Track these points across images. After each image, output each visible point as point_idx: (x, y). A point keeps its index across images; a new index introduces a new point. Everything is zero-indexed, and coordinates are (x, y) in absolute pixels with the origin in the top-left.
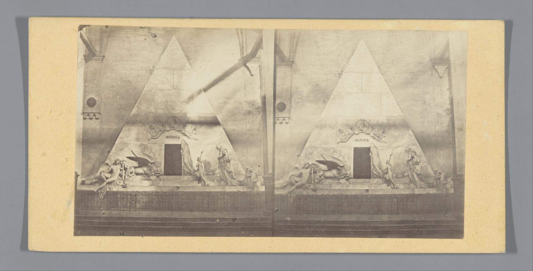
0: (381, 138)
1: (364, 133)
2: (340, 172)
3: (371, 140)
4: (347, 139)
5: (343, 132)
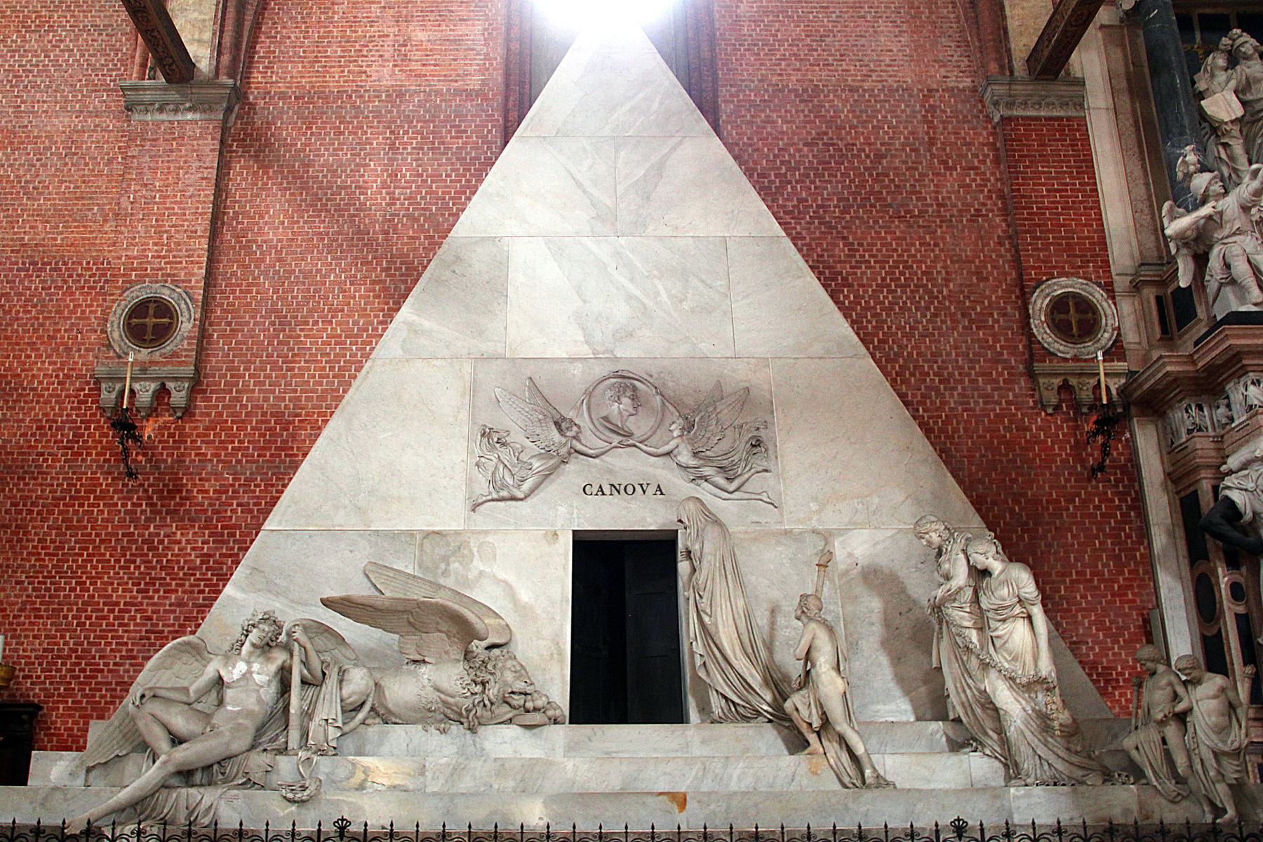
0: (746, 476)
1: (635, 446)
2: (484, 676)
3: (680, 485)
5: (504, 444)
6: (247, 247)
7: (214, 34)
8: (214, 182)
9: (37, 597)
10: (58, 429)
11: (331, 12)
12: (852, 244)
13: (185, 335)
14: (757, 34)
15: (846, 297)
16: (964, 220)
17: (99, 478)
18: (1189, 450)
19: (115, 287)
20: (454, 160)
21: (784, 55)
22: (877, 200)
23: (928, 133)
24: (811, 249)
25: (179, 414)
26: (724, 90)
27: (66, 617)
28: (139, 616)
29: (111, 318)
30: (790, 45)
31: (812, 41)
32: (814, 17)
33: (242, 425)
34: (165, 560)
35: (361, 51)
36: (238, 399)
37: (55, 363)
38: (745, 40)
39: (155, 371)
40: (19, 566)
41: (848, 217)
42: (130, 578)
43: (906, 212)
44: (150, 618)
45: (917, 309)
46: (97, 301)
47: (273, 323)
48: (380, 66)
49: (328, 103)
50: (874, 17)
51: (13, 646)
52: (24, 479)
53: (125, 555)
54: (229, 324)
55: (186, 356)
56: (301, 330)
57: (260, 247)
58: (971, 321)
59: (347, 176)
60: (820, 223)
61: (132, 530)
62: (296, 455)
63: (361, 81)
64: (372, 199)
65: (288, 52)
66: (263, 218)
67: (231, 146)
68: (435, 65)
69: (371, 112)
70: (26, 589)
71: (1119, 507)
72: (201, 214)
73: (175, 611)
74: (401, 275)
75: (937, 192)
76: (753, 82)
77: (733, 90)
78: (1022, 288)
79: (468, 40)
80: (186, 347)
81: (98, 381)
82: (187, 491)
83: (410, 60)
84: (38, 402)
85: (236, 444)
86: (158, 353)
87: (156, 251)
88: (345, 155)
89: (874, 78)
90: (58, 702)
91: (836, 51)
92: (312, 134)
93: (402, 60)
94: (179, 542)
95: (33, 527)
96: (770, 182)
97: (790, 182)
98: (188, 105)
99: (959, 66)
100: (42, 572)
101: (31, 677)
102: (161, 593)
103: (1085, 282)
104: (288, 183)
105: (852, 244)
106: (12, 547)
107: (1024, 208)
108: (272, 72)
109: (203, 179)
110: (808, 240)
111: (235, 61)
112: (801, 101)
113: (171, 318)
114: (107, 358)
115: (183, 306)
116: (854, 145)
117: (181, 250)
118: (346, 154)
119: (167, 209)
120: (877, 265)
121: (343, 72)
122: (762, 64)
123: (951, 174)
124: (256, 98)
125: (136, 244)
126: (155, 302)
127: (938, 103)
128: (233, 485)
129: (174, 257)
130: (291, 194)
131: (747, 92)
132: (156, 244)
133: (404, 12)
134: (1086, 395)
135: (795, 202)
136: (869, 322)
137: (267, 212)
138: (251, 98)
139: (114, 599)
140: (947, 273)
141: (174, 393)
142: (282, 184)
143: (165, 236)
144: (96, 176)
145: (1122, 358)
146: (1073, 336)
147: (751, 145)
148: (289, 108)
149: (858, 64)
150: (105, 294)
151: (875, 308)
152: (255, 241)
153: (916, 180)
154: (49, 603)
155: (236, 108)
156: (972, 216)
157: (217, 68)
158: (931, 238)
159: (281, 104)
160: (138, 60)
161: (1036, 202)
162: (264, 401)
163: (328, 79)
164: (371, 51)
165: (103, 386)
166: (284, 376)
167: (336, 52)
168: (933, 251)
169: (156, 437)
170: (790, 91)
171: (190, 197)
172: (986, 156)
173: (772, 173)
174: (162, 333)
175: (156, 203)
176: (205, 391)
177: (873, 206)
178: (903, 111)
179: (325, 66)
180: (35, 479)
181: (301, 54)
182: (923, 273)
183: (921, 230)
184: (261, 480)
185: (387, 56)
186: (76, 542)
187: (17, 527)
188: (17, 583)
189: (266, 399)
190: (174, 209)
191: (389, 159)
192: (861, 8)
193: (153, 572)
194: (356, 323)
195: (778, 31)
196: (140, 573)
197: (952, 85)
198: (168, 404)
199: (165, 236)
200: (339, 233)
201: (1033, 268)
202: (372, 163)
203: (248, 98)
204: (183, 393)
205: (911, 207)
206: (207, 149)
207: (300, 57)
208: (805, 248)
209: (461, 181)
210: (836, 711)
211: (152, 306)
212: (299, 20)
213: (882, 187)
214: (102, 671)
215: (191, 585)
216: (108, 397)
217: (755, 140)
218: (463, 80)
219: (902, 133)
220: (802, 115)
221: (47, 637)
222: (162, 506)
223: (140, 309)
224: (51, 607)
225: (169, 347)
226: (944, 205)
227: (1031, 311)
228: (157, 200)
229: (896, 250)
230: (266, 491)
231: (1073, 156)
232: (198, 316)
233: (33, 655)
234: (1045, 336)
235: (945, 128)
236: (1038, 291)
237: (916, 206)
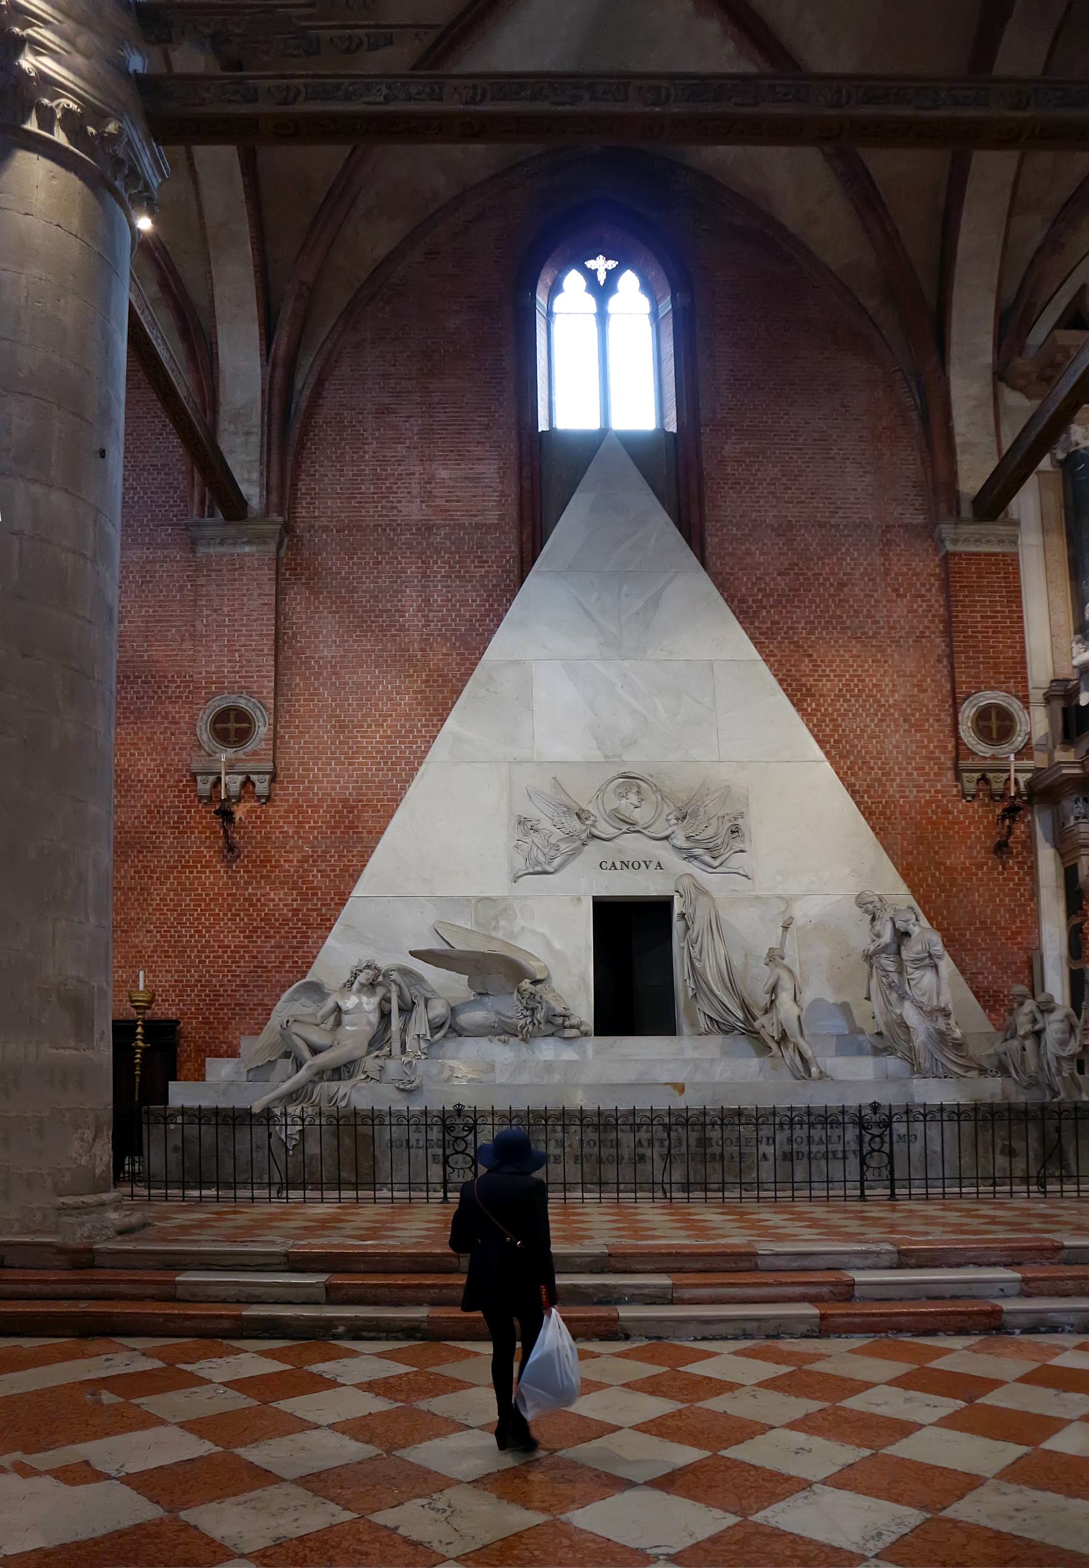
4: (557, 862)
6: (306, 663)
7: (261, 474)
8: (273, 607)
9: (164, 942)
10: (164, 813)
11: (361, 451)
12: (816, 661)
13: (263, 737)
14: (740, 474)
15: (809, 705)
16: (911, 640)
17: (203, 852)
18: (1074, 832)
19: (199, 698)
20: (478, 587)
21: (763, 493)
22: (838, 623)
23: (884, 565)
24: (781, 665)
25: (263, 801)
26: (710, 524)
27: (189, 957)
28: (247, 955)
29: (199, 723)
30: (768, 484)
31: (787, 480)
32: (790, 458)
33: (315, 808)
34: (263, 914)
35: (391, 488)
36: (310, 788)
37: (155, 760)
38: (729, 479)
39: (240, 767)
40: (147, 919)
41: (813, 637)
42: (236, 928)
43: (863, 634)
44: (255, 957)
45: (867, 716)
46: (184, 708)
47: (334, 727)
48: (409, 502)
49: (365, 536)
50: (842, 459)
51: (151, 978)
52: (142, 852)
53: (231, 910)
54: (297, 727)
55: (265, 754)
56: (358, 732)
57: (317, 662)
58: (912, 725)
59: (387, 601)
60: (790, 643)
61: (234, 891)
62: (361, 833)
63: (393, 516)
64: (410, 621)
65: (327, 490)
66: (318, 638)
67: (284, 574)
68: (458, 501)
69: (404, 544)
70: (155, 936)
71: (1017, 873)
72: (266, 635)
73: (274, 952)
74: (438, 686)
75: (890, 617)
76: (735, 517)
77: (718, 524)
78: (954, 699)
79: (486, 478)
80: (264, 747)
81: (194, 775)
82: (276, 861)
83: (436, 497)
84: (145, 791)
85: (312, 824)
86: (241, 752)
87: (231, 667)
88: (384, 582)
89: (840, 514)
90: (191, 1018)
91: (808, 489)
92: (354, 563)
93: (428, 496)
94: (273, 900)
95: (155, 890)
96: (750, 607)
97: (765, 608)
98: (245, 540)
99: (913, 504)
100: (166, 924)
101: (168, 1000)
102: (263, 938)
103: (1006, 694)
104: (336, 607)
105: (816, 661)
106: (140, 905)
107: (961, 632)
108: (315, 508)
109: (264, 604)
110: (778, 658)
111: (282, 498)
112: (776, 535)
113: (250, 722)
114: (199, 756)
115: (258, 713)
116: (821, 574)
117: (252, 666)
118: (385, 582)
119: (236, 631)
120: (836, 679)
121: (377, 507)
122: (743, 502)
123: (902, 601)
124: (302, 531)
125: (213, 662)
126: (235, 710)
127: (894, 538)
128: (312, 856)
129: (246, 672)
130: (340, 617)
131: (730, 527)
132: (229, 661)
133: (427, 452)
134: (997, 786)
135: (769, 625)
136: (827, 726)
137: (321, 632)
138: (298, 531)
139: (226, 943)
140: (894, 685)
141: (257, 784)
142: (331, 607)
143: (237, 654)
144: (171, 601)
145: (1030, 757)
146: (992, 739)
147: (732, 574)
148: (332, 540)
149: (826, 501)
150: (192, 702)
151: (832, 714)
152: (313, 658)
153: (872, 606)
154: (174, 947)
155: (286, 541)
156: (917, 637)
157: (267, 505)
158: (882, 656)
159: (324, 537)
160: (196, 498)
161: (971, 627)
162: (332, 790)
163: (364, 513)
164: (399, 488)
165: (199, 778)
166: (347, 770)
167: (369, 489)
168: (883, 667)
169: (246, 819)
170: (767, 526)
171: (255, 620)
172: (933, 585)
173: (750, 599)
174: (242, 736)
175: (227, 626)
176: (282, 782)
177: (835, 628)
178: (863, 545)
179: (360, 502)
180: (152, 852)
181: (339, 491)
182: (874, 685)
183: (874, 649)
184: (335, 852)
185: (415, 492)
186: (191, 900)
187: (141, 889)
188: (148, 932)
189: (334, 788)
190: (241, 631)
191: (423, 586)
192: (832, 449)
193: (255, 923)
194: (402, 726)
195: (758, 470)
196: (245, 924)
197: (906, 521)
198: (254, 793)
199: (237, 654)
200: (383, 650)
201: (965, 682)
202: (408, 590)
203: (295, 532)
204: (266, 784)
205: (866, 629)
206: (266, 578)
207: (338, 493)
208: (776, 664)
209: (485, 606)
210: (793, 1028)
211: (232, 714)
212: (334, 458)
213: (843, 612)
214: (222, 996)
215: (286, 932)
216: (204, 786)
217: (736, 569)
218: (483, 515)
219: (861, 564)
220: (776, 548)
221: (176, 971)
222: (256, 872)
223: (222, 716)
224: (177, 950)
225: (250, 746)
226: (894, 628)
227: (960, 719)
228: (227, 623)
229: (851, 666)
230: (339, 860)
231: (1006, 587)
232: (272, 721)
233: (167, 984)
234: (970, 739)
235: (899, 560)
236: (967, 702)
237: (871, 629)
